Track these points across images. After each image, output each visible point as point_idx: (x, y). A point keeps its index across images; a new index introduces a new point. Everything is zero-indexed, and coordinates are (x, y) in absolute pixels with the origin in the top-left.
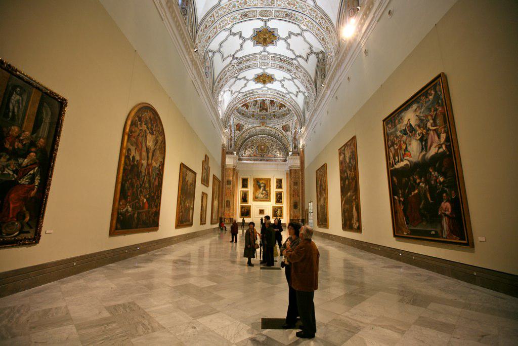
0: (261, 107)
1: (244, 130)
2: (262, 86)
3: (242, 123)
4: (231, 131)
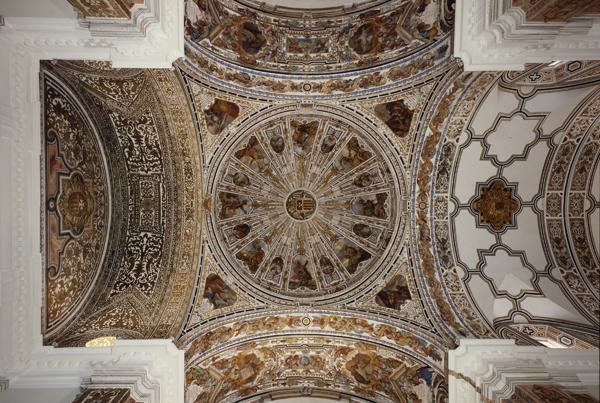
0: (229, 196)
1: (205, 129)
2: (464, 199)
3: (232, 129)
4: (229, 77)
